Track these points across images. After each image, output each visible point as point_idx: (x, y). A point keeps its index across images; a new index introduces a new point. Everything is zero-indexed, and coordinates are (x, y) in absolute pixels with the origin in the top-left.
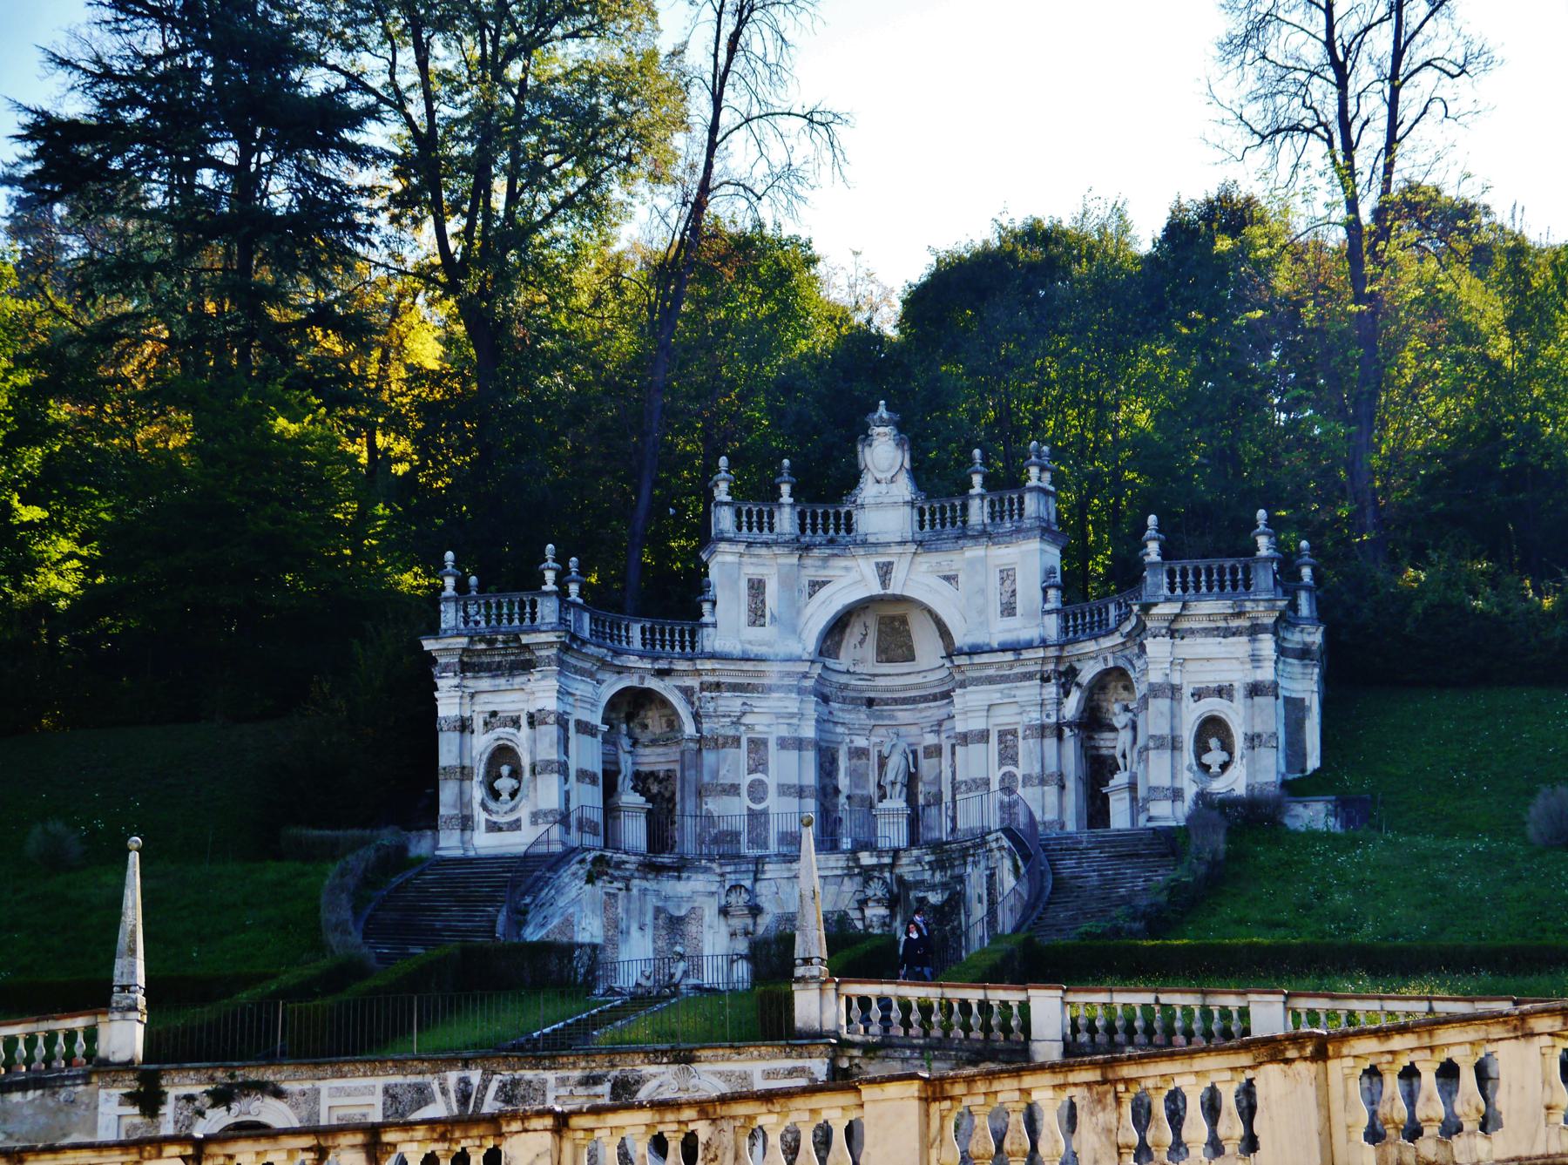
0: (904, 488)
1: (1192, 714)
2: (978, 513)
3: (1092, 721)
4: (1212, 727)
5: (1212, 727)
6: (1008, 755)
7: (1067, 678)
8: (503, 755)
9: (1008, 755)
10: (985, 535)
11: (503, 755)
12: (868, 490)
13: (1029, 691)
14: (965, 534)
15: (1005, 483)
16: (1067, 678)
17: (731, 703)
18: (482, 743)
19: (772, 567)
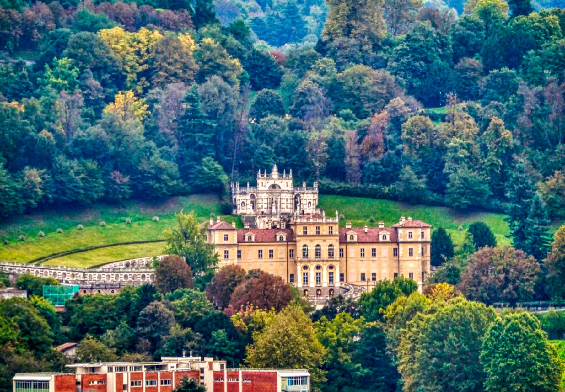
0: (277, 173)
1: (308, 201)
2: (284, 176)
3: (296, 198)
4: (310, 203)
5: (310, 203)
6: (287, 200)
7: (293, 193)
8: (243, 202)
9: (287, 200)
10: (285, 179)
11: (243, 202)
12: (273, 173)
13: (289, 195)
14: (283, 179)
15: (288, 173)
16: (293, 193)
17: (260, 195)
18: (241, 201)
19: (264, 181)
